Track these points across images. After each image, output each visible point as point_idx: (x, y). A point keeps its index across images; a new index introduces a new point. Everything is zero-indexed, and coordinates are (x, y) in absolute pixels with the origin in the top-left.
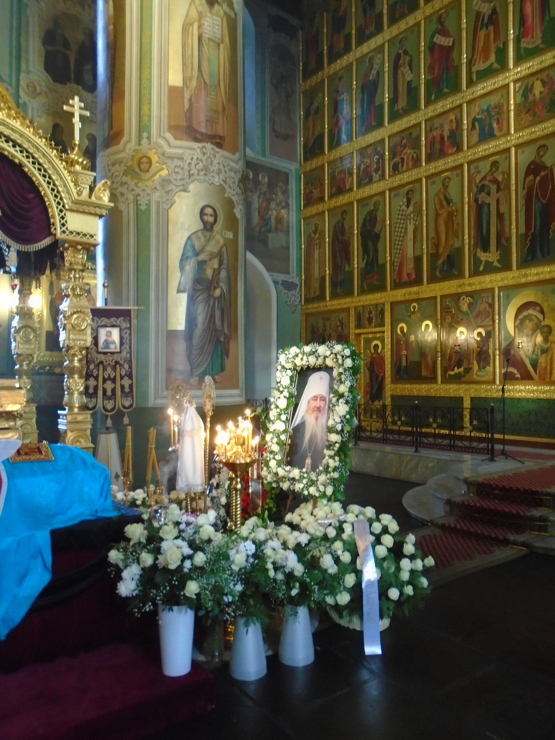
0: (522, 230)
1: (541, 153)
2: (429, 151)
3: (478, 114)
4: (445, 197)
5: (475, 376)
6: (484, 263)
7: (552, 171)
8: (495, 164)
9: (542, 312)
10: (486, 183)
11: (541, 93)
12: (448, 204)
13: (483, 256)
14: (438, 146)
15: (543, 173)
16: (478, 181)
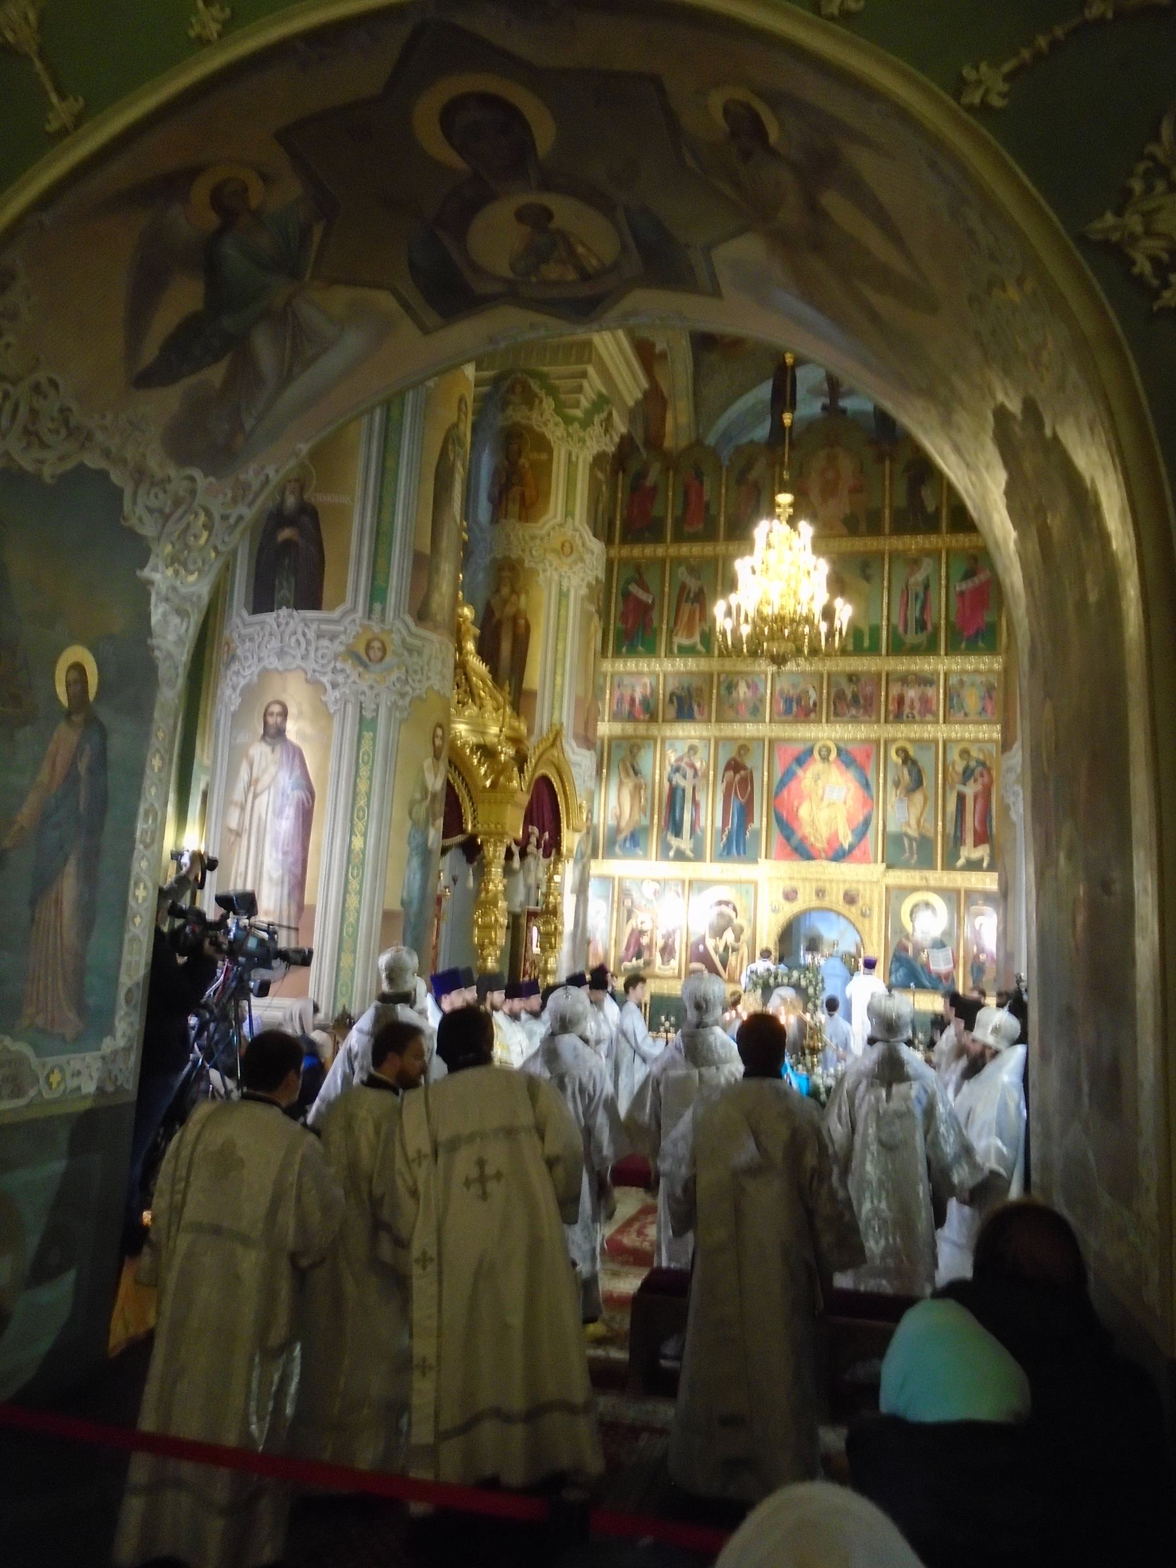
0: (719, 823)
1: (742, 752)
2: (615, 708)
3: (678, 689)
4: (633, 767)
5: (657, 971)
6: (674, 848)
7: (751, 772)
8: (693, 749)
9: (735, 909)
10: (683, 765)
11: (745, 693)
12: (636, 773)
13: (674, 842)
14: (626, 707)
15: (742, 772)
16: (673, 760)
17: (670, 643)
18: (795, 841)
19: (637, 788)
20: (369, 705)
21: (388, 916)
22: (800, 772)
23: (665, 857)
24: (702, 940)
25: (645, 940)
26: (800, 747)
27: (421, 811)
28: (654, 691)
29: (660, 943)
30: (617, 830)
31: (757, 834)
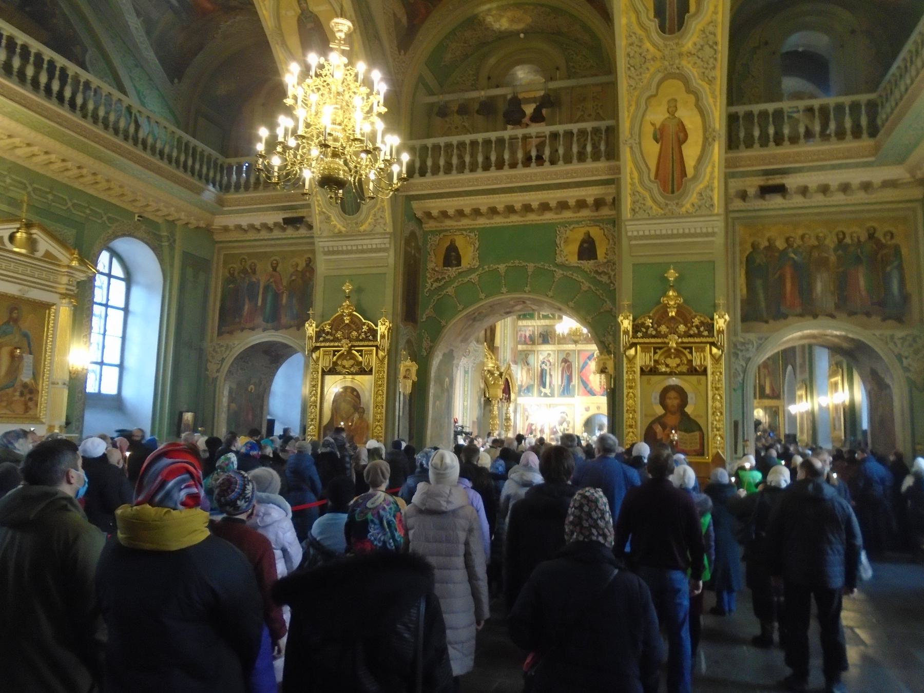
0: (560, 383)
8: (549, 354)
14: (523, 339)
17: (539, 314)
18: (588, 389)
19: (529, 370)
20: (467, 367)
21: (474, 422)
22: (589, 363)
23: (541, 396)
24: (555, 427)
25: (533, 427)
26: (589, 354)
27: (479, 394)
28: (533, 332)
29: (539, 428)
30: (521, 386)
31: (574, 386)
